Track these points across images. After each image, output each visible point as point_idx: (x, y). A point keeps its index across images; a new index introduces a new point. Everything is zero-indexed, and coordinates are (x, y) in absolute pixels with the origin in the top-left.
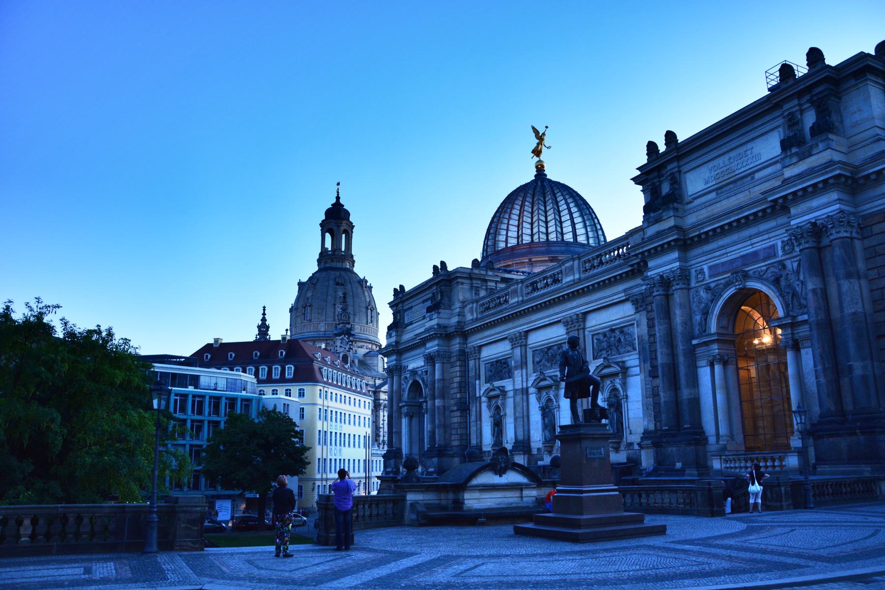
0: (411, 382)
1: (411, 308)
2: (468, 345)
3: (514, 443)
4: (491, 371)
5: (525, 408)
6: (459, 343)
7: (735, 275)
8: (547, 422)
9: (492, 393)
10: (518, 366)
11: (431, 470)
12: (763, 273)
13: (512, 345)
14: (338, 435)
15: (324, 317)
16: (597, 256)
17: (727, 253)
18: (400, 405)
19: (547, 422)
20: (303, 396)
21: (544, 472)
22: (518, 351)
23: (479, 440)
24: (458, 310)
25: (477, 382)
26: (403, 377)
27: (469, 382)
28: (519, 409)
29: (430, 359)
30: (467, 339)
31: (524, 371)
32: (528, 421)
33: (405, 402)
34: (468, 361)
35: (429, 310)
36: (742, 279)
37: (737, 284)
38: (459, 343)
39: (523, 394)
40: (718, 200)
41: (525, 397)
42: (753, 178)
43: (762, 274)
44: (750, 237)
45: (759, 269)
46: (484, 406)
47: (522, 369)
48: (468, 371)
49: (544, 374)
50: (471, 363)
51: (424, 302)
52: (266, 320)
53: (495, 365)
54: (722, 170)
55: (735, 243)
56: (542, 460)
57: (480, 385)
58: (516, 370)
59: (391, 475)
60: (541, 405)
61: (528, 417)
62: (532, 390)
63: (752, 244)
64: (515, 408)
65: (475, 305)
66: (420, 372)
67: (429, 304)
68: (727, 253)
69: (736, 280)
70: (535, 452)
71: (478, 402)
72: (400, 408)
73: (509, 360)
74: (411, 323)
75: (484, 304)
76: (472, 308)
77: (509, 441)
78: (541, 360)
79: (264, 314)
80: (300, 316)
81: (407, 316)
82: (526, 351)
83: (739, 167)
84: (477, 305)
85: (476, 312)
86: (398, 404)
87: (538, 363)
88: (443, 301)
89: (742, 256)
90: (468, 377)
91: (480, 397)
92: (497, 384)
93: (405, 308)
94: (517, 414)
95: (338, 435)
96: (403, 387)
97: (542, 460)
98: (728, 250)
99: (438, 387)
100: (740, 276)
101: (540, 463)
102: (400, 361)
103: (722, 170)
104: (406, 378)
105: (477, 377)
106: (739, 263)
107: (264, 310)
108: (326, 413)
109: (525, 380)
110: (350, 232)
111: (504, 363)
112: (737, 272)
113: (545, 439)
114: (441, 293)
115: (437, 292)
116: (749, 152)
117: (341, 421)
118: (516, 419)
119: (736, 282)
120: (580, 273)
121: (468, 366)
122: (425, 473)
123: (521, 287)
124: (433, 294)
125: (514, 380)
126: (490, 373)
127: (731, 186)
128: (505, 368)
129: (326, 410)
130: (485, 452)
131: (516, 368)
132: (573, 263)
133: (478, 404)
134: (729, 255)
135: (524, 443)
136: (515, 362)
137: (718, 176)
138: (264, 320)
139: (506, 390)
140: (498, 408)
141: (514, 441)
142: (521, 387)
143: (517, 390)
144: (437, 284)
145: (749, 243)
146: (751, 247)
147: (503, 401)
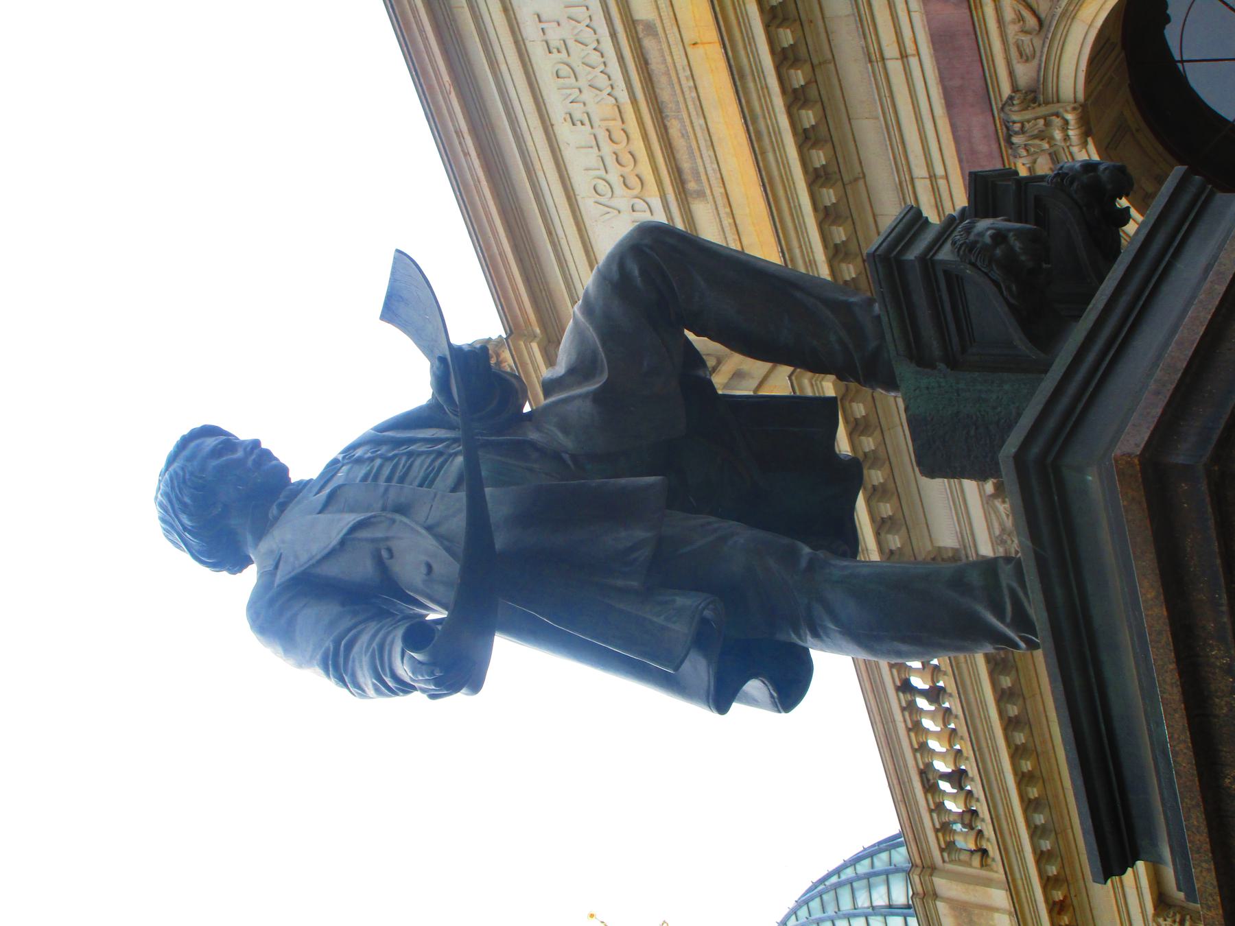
7: (1015, 140)
12: (1026, 14)
16: (930, 788)
17: (932, 177)
36: (1043, 110)
37: (1058, 135)
40: (719, 190)
42: (650, 28)
43: (1032, 22)
44: (874, 58)
45: (1012, 30)
54: (610, 160)
55: (893, 127)
63: (904, 56)
68: (932, 177)
69: (1041, 136)
83: (602, 81)
89: (949, 105)
98: (920, 171)
100: (1028, 115)
103: (610, 160)
106: (978, 125)
112: (1007, 124)
116: (554, 35)
119: (1051, 139)
120: (988, 883)
127: (674, 131)
132: (949, 901)
134: (939, 171)
137: (633, 181)
145: (895, 67)
146: (914, 61)
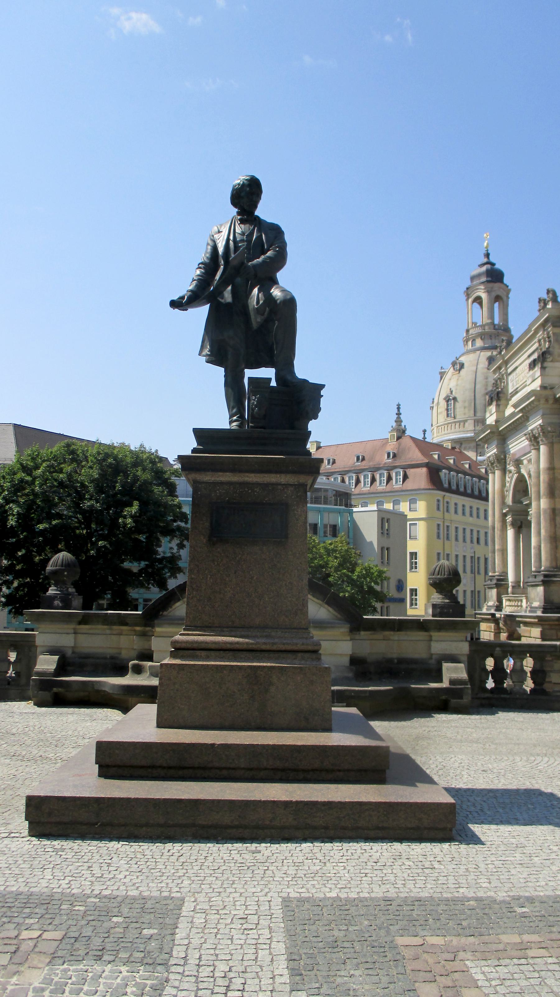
0: (516, 476)
1: (516, 368)
11: (536, 604)
15: (472, 412)
18: (504, 511)
29: (534, 440)
33: (509, 506)
35: (532, 365)
51: (529, 356)
52: (402, 421)
59: (493, 611)
66: (525, 462)
67: (535, 356)
72: (505, 515)
74: (516, 392)
79: (399, 414)
80: (441, 413)
81: (512, 381)
86: (502, 509)
93: (509, 370)
95: (468, 560)
104: (510, 472)
107: (399, 408)
108: (448, 530)
110: (505, 298)
115: (543, 338)
122: (529, 609)
124: (539, 341)
129: (448, 527)
138: (399, 421)
144: (543, 325)
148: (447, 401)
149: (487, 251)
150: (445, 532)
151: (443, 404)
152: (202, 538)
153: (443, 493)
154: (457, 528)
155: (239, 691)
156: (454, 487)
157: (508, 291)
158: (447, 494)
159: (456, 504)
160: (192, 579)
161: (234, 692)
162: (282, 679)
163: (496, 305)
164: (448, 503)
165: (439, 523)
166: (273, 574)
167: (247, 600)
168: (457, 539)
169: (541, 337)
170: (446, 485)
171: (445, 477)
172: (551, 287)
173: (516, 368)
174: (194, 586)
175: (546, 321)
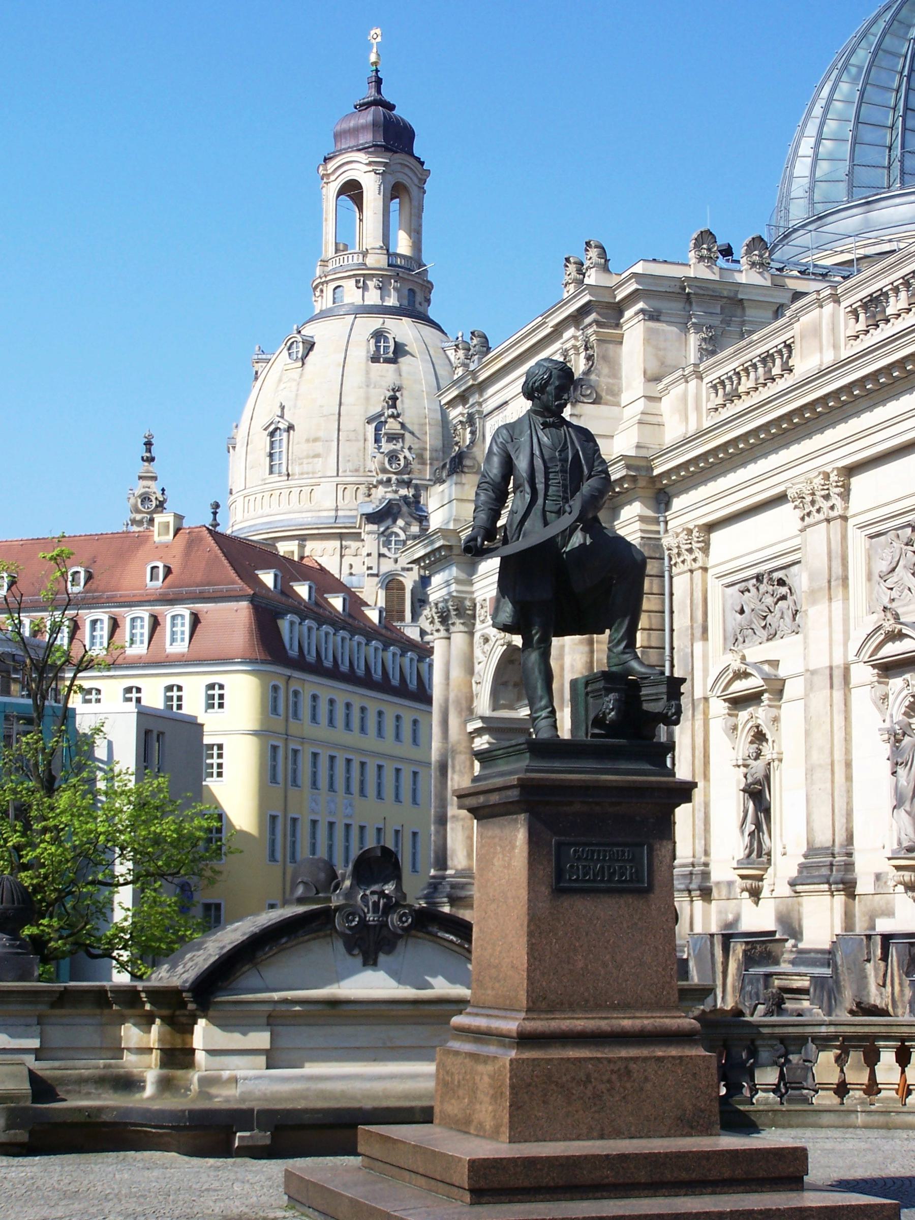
1: (506, 403)
2: (671, 525)
3: (806, 856)
4: (742, 612)
5: (839, 735)
6: (642, 519)
8: (903, 782)
9: (740, 686)
10: (820, 589)
13: (803, 519)
14: (339, 832)
19: (903, 782)
20: (221, 706)
21: (885, 957)
22: (818, 538)
23: (700, 849)
24: (641, 405)
25: (698, 646)
26: (477, 636)
27: (672, 648)
28: (820, 738)
30: (668, 506)
31: (837, 605)
32: (849, 778)
33: (482, 718)
34: (671, 578)
38: (642, 519)
39: (832, 687)
41: (838, 695)
46: (717, 727)
47: (830, 599)
48: (672, 612)
49: (897, 617)
50: (681, 584)
53: (753, 590)
56: (889, 913)
57: (705, 657)
58: (814, 602)
60: (887, 725)
61: (848, 765)
62: (864, 674)
64: (807, 733)
65: (693, 383)
70: (864, 886)
71: (699, 716)
73: (795, 569)
75: (722, 383)
76: (686, 391)
77: (788, 850)
78: (893, 570)
82: (844, 537)
84: (698, 388)
85: (698, 408)
87: (884, 578)
88: (593, 377)
90: (672, 630)
91: (706, 699)
92: (756, 652)
94: (815, 757)
95: (339, 832)
96: (477, 668)
97: (889, 913)
99: (572, 666)
101: (884, 926)
102: (471, 584)
105: (698, 632)
107: (148, 444)
109: (838, 636)
110: (414, 191)
111: (781, 582)
113: (900, 843)
114: (586, 349)
117: (348, 790)
118: (810, 771)
121: (671, 594)
123: (834, 316)
125: (805, 638)
126: (738, 615)
128: (784, 598)
130: (718, 883)
131: (813, 594)
133: (699, 723)
135: (833, 855)
136: (812, 578)
139: (782, 673)
140: (759, 737)
141: (804, 849)
142: (828, 664)
143: (813, 673)
144: (576, 318)
147: (774, 712)
148: (272, 434)
149: (377, 71)
150: (290, 766)
151: (262, 441)
152: (543, 889)
153: (288, 672)
154: (315, 755)
155: (608, 1090)
156: (344, 668)
157: (423, 176)
158: (297, 674)
159: (315, 698)
160: (533, 944)
161: (602, 1092)
162: (659, 1073)
163: (395, 204)
164: (296, 693)
165: (276, 743)
166: (633, 935)
167: (602, 972)
168: (314, 785)
169: (568, 345)
170: (294, 653)
171: (291, 631)
172: (595, 239)
173: (506, 403)
174: (536, 954)
175: (584, 311)
